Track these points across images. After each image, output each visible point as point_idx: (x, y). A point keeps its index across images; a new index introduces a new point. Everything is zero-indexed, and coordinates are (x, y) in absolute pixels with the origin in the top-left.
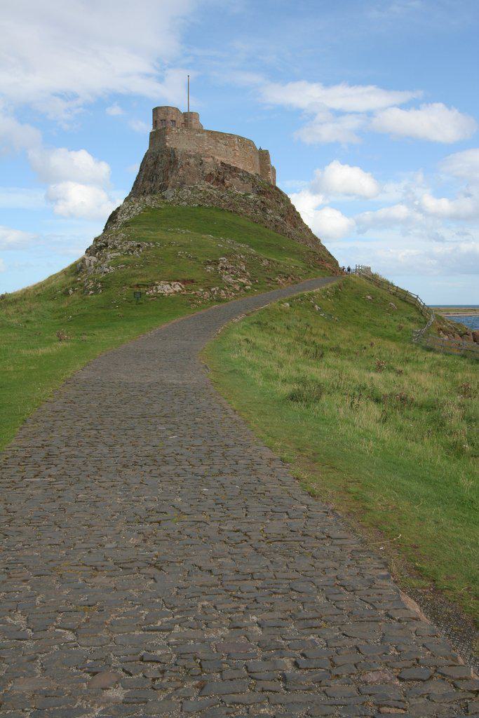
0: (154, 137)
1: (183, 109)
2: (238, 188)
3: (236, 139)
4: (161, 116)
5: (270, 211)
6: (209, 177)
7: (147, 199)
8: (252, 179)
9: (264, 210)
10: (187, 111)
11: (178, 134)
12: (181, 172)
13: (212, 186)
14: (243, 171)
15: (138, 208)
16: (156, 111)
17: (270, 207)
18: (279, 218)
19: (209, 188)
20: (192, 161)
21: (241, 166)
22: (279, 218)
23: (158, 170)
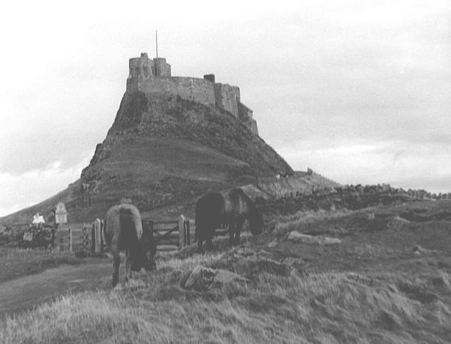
0: (129, 82)
1: (151, 56)
2: (194, 117)
3: (192, 80)
4: (135, 64)
5: (217, 134)
6: (169, 112)
7: (125, 133)
8: (208, 109)
9: (213, 134)
10: (155, 57)
11: (147, 81)
12: (150, 110)
13: (173, 118)
14: (199, 104)
15: (119, 140)
16: (131, 61)
17: (217, 131)
18: (225, 139)
19: (171, 120)
20: (157, 101)
21: (197, 100)
22: (225, 139)
23: (133, 107)
